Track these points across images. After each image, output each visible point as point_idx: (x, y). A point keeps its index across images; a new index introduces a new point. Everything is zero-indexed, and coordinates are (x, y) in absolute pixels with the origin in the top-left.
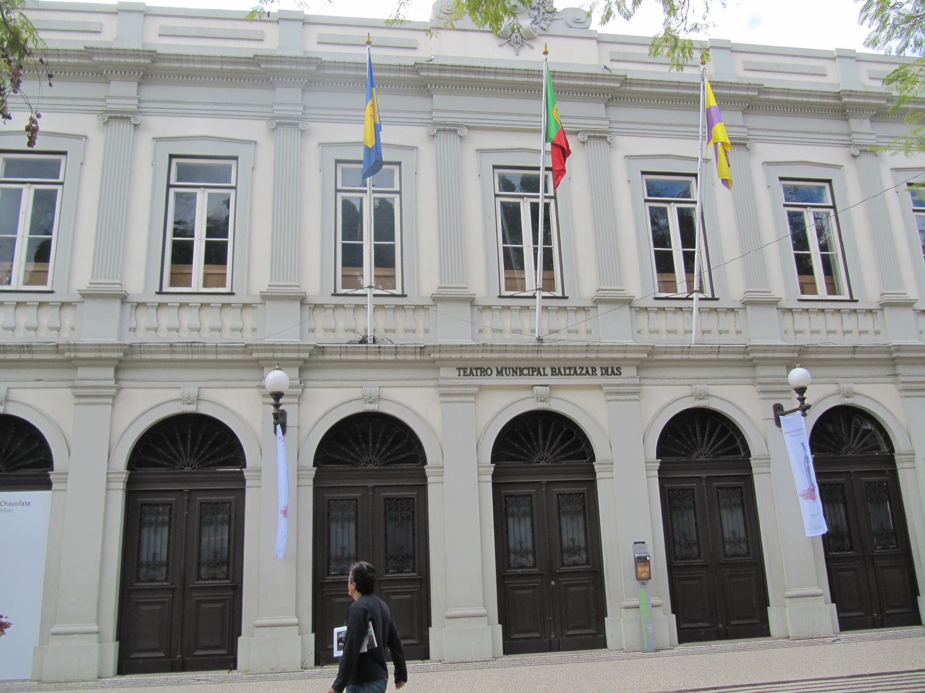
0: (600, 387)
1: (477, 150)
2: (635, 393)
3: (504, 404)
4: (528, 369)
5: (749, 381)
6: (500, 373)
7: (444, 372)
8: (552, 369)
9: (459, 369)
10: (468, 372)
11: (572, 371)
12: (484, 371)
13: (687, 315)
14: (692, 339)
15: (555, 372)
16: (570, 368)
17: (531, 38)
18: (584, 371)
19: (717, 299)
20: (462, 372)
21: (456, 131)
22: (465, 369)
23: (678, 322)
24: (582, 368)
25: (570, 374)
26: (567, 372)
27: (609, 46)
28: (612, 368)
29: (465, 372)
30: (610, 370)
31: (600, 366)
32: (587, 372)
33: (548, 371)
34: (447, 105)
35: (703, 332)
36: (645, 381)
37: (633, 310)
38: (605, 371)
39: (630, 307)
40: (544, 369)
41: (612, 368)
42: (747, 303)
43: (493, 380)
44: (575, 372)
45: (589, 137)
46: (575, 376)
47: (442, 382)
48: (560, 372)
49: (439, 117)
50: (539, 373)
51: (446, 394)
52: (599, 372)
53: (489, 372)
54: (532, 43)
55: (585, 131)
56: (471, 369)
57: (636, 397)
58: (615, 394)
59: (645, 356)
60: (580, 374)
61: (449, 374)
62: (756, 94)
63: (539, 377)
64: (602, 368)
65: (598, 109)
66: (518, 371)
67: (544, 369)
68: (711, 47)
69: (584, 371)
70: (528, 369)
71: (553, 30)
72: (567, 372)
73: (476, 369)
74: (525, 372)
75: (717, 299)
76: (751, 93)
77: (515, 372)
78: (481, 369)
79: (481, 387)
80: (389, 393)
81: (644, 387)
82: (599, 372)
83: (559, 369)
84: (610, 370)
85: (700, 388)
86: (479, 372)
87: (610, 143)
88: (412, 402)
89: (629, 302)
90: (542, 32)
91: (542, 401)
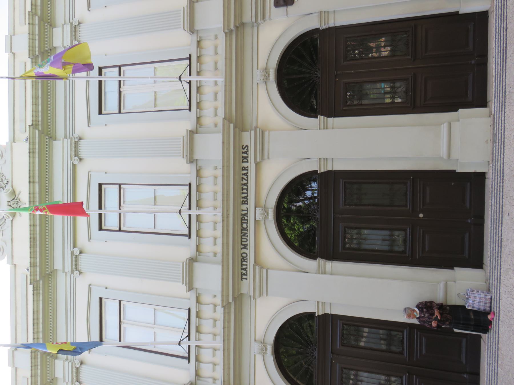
0: (257, 165)
1: (89, 241)
2: (263, 133)
3: (270, 247)
4: (242, 223)
5: (255, 29)
6: (245, 247)
7: (244, 291)
8: (242, 204)
9: (242, 279)
10: (244, 272)
11: (245, 187)
12: (244, 259)
13: (203, 84)
14: (221, 80)
15: (245, 202)
16: (243, 189)
17: (14, 192)
18: (245, 177)
19: (190, 55)
20: (244, 277)
21: (76, 257)
22: (242, 274)
23: (208, 91)
24: (243, 178)
25: (247, 189)
26: (245, 191)
27: (17, 132)
28: (243, 153)
29: (244, 274)
30: (244, 155)
31: (241, 162)
32: (246, 174)
33: (244, 207)
34: (61, 260)
35: (216, 69)
36: (254, 125)
37: (200, 130)
38: (245, 159)
39: (197, 133)
40: (242, 210)
41: (243, 153)
42: (192, 30)
43: (251, 252)
44: (246, 184)
45: (76, 156)
46: (249, 185)
47: (251, 294)
48: (246, 197)
49: (68, 267)
50: (246, 215)
51: (261, 290)
52: (245, 165)
53: (244, 255)
54: (17, 193)
55: (72, 159)
56: (242, 269)
57: (266, 133)
58: (263, 156)
59: (232, 125)
60: (247, 180)
61: (247, 287)
62: (37, 17)
63: (248, 215)
64: (243, 162)
65: (57, 145)
66: (244, 232)
67: (242, 210)
68: (11, 51)
69: (245, 177)
70: (242, 223)
71: (8, 177)
72: (245, 191)
73: (242, 265)
74: (245, 226)
75: (190, 55)
76: (37, 22)
77: (245, 235)
78: (242, 261)
79: (256, 262)
80: (260, 333)
81: (259, 125)
82: (245, 165)
83: (242, 198)
84: (244, 155)
85: (258, 76)
86: (244, 263)
87: (80, 139)
88: (267, 316)
89: (192, 133)
90: (10, 183)
91: (268, 214)
